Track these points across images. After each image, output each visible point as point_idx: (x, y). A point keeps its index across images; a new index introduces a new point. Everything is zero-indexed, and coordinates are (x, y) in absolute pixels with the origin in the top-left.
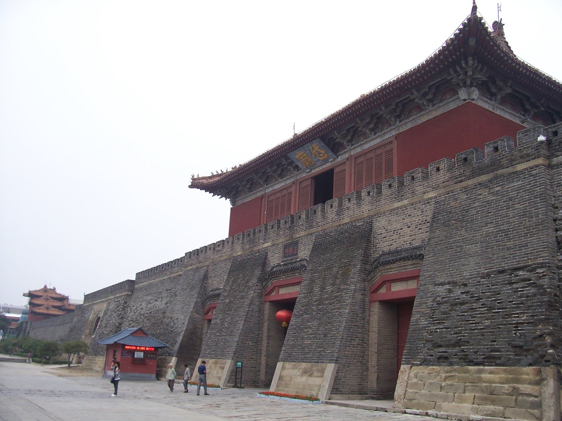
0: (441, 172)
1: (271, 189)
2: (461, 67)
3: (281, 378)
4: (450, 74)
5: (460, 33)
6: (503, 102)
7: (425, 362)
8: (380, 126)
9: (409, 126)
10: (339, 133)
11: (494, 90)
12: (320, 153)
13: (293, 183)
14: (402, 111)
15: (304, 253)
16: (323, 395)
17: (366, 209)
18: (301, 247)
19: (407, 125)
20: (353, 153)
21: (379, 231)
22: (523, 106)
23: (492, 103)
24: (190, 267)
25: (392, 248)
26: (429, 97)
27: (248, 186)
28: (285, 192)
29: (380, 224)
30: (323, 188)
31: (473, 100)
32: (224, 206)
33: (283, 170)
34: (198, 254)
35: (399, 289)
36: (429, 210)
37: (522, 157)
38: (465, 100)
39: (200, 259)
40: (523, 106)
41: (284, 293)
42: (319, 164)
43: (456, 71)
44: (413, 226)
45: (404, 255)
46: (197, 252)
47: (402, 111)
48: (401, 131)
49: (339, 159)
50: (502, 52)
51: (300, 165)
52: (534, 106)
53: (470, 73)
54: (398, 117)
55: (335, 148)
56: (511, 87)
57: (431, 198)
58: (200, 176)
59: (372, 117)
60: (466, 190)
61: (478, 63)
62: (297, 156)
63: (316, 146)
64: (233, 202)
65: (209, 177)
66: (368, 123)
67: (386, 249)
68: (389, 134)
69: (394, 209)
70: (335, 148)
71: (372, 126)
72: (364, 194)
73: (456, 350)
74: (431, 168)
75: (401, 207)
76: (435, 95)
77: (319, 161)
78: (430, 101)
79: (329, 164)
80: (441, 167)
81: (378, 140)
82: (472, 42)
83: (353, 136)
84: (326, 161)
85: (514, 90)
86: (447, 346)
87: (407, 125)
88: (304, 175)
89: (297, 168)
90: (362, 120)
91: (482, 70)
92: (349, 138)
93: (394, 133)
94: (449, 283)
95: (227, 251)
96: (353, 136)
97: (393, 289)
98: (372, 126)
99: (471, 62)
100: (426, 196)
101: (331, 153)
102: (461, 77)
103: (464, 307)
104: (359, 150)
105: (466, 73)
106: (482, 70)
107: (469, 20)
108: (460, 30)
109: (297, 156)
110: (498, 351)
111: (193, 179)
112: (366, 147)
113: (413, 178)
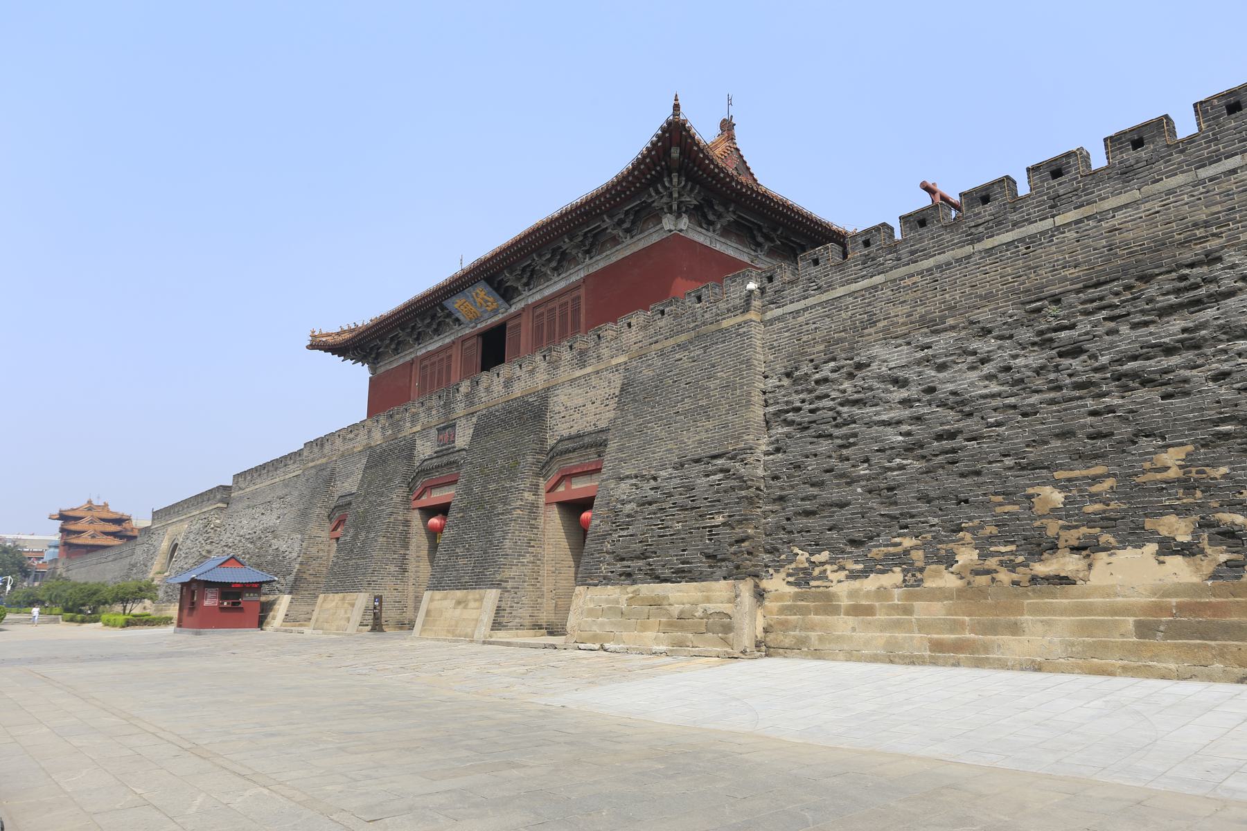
0: (634, 328)
1: (424, 351)
2: (664, 186)
3: (428, 613)
4: (650, 196)
5: (658, 141)
6: (726, 232)
7: (606, 581)
8: (565, 263)
9: (602, 265)
10: (511, 274)
11: (711, 217)
12: (486, 301)
13: (453, 342)
14: (592, 245)
15: (463, 438)
16: (484, 630)
17: (540, 380)
18: (459, 430)
19: (599, 263)
20: (530, 301)
21: (557, 409)
22: (754, 238)
23: (710, 234)
24: (311, 464)
25: (573, 432)
26: (626, 226)
27: (393, 346)
28: (443, 355)
29: (561, 400)
30: (493, 348)
31: (681, 231)
32: (357, 375)
33: (439, 324)
34: (322, 445)
35: (579, 487)
36: (617, 380)
37: (729, 310)
38: (670, 231)
39: (326, 451)
40: (754, 238)
41: (438, 496)
42: (486, 315)
43: (657, 192)
45: (587, 440)
46: (320, 443)
47: (592, 245)
48: (592, 270)
49: (513, 310)
50: (717, 166)
51: (461, 318)
52: (768, 238)
53: (676, 195)
54: (588, 252)
55: (507, 294)
56: (734, 212)
57: (620, 364)
58: (324, 332)
59: (554, 252)
60: (662, 354)
61: (686, 181)
62: (456, 306)
63: (481, 292)
64: (373, 370)
65: (338, 334)
66: (549, 260)
67: (566, 433)
68: (576, 275)
69: (575, 379)
70: (507, 294)
71: (554, 264)
73: (641, 563)
74: (622, 323)
75: (584, 376)
76: (633, 223)
77: (486, 311)
78: (628, 231)
79: (501, 316)
80: (633, 321)
82: (675, 153)
83: (531, 277)
84: (495, 312)
85: (740, 217)
86: (631, 559)
87: (599, 263)
89: (457, 320)
90: (540, 256)
91: (692, 190)
92: (525, 280)
93: (582, 274)
94: (636, 477)
95: (360, 442)
96: (531, 277)
97: (574, 487)
98: (554, 264)
99: (675, 180)
100: (614, 362)
101: (501, 301)
102: (665, 200)
103: (654, 507)
104: (538, 297)
105: (671, 195)
106: (692, 190)
107: (669, 123)
108: (657, 136)
109: (456, 304)
110: (688, 563)
111: (314, 337)
112: (547, 292)
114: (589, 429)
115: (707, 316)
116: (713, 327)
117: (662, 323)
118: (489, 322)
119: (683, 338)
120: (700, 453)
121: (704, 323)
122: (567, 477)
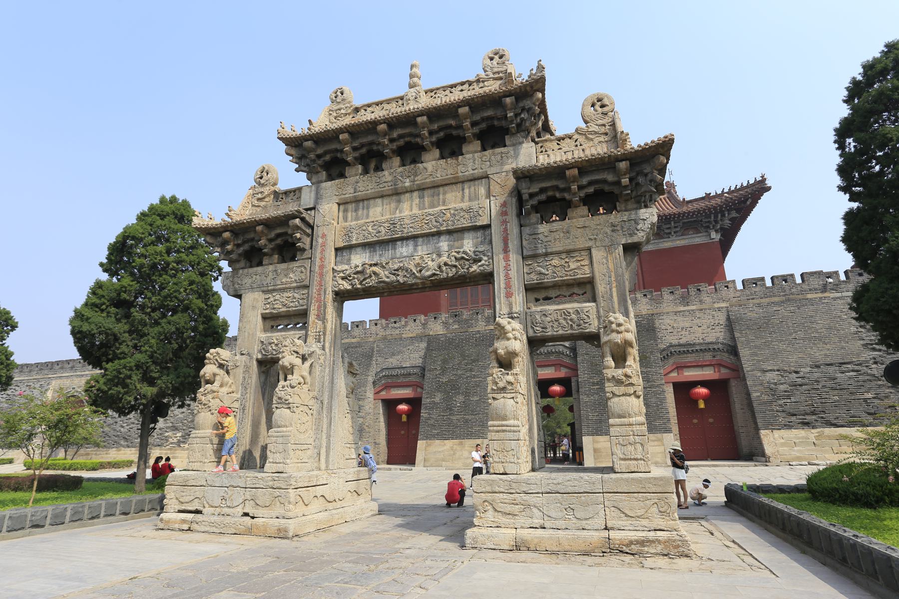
25: (682, 341)
37: (810, 290)
44: (705, 327)
45: (698, 348)
67: (675, 342)
97: (686, 374)
113: (699, 290)
115: (793, 290)
116: (800, 297)
117: (757, 289)
119: (776, 299)
120: (828, 360)
121: (792, 294)
122: (680, 368)
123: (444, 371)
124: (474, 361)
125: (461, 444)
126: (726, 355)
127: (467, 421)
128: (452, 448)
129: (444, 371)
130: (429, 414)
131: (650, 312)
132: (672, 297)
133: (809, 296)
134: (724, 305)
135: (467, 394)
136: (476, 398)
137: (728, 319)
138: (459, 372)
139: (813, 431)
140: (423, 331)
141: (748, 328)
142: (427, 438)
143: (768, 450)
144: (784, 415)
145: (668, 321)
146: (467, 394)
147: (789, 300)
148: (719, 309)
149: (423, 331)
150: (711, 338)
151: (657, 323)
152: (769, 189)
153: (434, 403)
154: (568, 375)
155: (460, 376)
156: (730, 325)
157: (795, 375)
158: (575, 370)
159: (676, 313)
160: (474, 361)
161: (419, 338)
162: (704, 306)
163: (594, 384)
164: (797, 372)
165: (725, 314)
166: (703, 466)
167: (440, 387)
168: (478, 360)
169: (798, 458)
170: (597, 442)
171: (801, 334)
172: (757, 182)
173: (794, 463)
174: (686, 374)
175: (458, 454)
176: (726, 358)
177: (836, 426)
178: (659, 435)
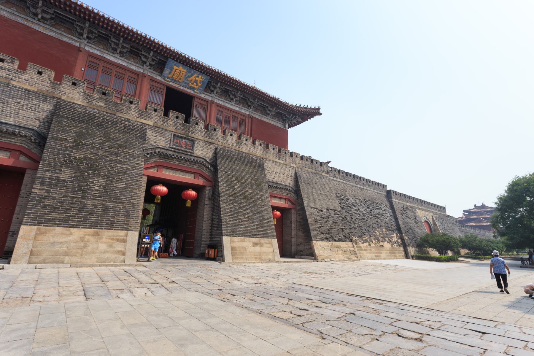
25: (275, 180)
44: (285, 175)
45: (281, 186)
67: (271, 180)
70: (208, 88)
72: (257, 142)
81: (237, 109)
88: (159, 78)
97: (273, 201)
112: (227, 105)
114: (281, 183)
118: (181, 88)
119: (313, 171)
123: (78, 145)
124: (121, 146)
125: (97, 234)
126: (293, 194)
127: (107, 208)
128: (82, 239)
129: (78, 145)
130: (49, 192)
131: (262, 156)
132: (273, 151)
133: (323, 174)
134: (294, 166)
135: (109, 178)
136: (121, 185)
137: (296, 174)
138: (101, 153)
139: (330, 243)
140: (51, 90)
141: (304, 182)
142: (40, 221)
143: (317, 253)
144: (319, 233)
145: (270, 166)
146: (109, 178)
147: (317, 173)
148: (292, 167)
149: (51, 90)
150: (287, 184)
151: (265, 164)
152: (320, 114)
153: (59, 180)
154: (205, 184)
155: (101, 158)
156: (296, 178)
157: (321, 212)
158: (214, 182)
159: (274, 162)
160: (121, 146)
161: (44, 97)
162: (286, 163)
163: (230, 195)
164: (322, 211)
165: (294, 171)
166: (288, 262)
167: (69, 163)
168: (126, 147)
169: (327, 258)
170: (234, 242)
171: (321, 192)
172: (315, 109)
173: (326, 260)
174: (273, 201)
175: (91, 247)
176: (292, 196)
177: (336, 241)
178: (270, 240)
